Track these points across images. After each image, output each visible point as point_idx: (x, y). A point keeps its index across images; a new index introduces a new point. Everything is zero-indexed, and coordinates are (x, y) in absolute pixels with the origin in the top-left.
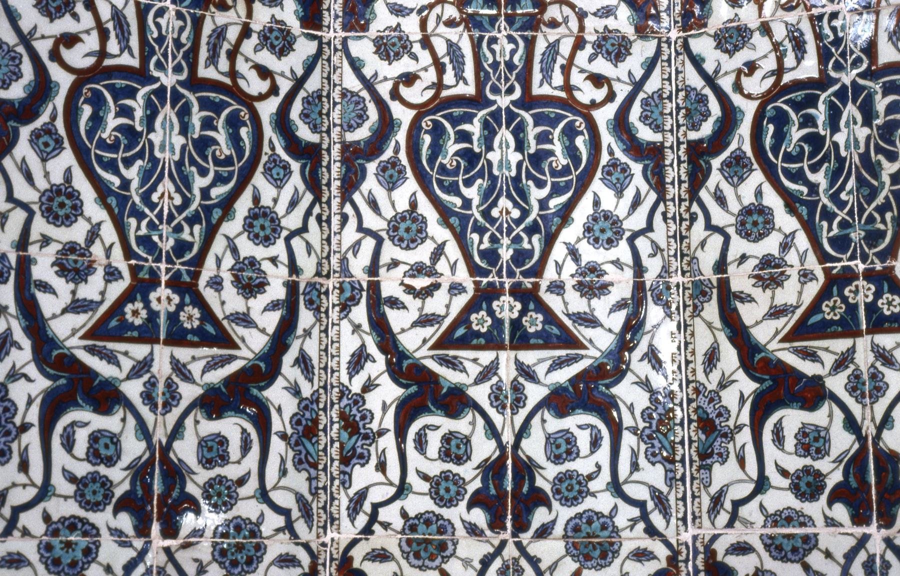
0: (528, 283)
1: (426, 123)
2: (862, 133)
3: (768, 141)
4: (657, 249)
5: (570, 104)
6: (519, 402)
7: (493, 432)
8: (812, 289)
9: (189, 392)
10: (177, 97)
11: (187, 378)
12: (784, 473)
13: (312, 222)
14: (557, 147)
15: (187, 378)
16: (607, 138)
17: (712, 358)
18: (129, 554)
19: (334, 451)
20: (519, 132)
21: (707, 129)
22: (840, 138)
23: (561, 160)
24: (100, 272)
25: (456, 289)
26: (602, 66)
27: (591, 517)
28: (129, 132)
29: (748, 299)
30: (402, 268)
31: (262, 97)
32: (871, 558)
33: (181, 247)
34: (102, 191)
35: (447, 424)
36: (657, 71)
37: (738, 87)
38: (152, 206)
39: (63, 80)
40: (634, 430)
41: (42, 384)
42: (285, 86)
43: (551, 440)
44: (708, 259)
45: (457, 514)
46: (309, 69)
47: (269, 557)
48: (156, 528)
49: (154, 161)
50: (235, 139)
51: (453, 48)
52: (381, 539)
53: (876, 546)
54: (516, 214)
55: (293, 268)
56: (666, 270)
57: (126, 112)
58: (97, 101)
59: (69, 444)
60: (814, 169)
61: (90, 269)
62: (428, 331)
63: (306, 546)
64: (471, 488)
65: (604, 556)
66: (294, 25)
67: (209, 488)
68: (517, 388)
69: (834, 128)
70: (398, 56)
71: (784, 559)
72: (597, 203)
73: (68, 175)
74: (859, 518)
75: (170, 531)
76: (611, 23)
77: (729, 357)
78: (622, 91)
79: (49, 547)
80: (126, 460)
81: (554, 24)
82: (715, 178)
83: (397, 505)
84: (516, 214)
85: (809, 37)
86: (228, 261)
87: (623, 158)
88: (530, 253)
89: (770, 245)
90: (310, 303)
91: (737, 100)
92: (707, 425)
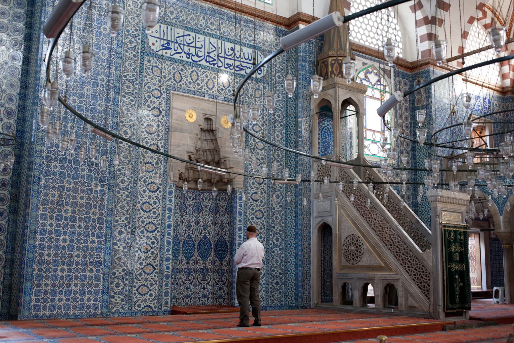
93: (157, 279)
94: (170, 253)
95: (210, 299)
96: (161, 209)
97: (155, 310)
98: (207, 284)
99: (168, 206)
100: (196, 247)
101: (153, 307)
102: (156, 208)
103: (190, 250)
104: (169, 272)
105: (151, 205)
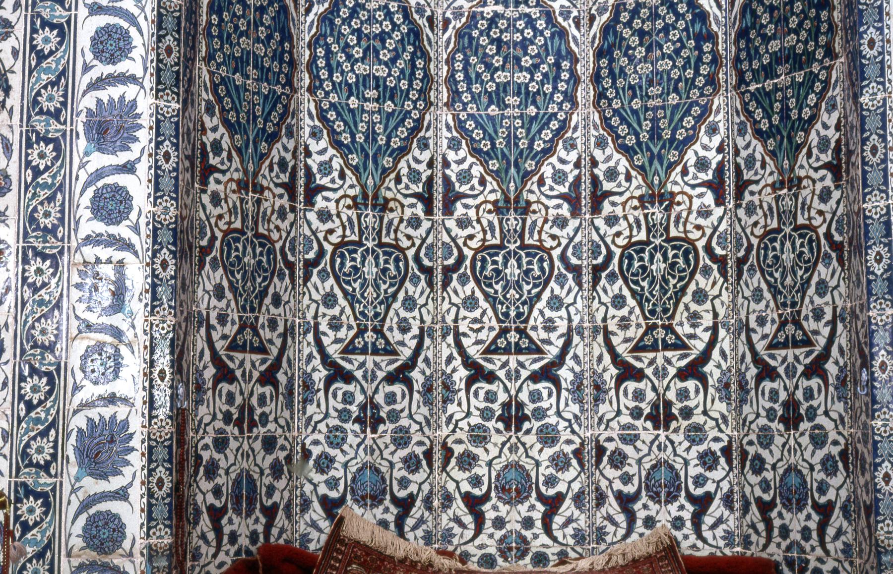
0: (522, 326)
1: (479, 257)
2: (663, 266)
3: (625, 267)
4: (578, 311)
5: (541, 248)
6: (518, 377)
7: (506, 390)
8: (641, 331)
9: (381, 375)
10: (374, 251)
11: (380, 369)
12: (627, 408)
13: (430, 300)
14: (536, 267)
15: (380, 369)
16: (557, 263)
17: (600, 359)
18: (359, 440)
19: (440, 398)
20: (519, 260)
21: (600, 260)
22: (654, 267)
23: (537, 273)
24: (345, 326)
25: (491, 329)
26: (556, 231)
27: (547, 426)
28: (355, 268)
29: (615, 334)
30: (468, 320)
31: (408, 248)
32: (660, 444)
33: (377, 315)
34: (345, 293)
35: (487, 387)
36: (579, 234)
37: (613, 242)
38: (365, 298)
39: (329, 248)
40: (567, 390)
41: (325, 373)
42: (418, 242)
43: (531, 394)
44: (599, 316)
45: (491, 424)
46: (428, 233)
47: (413, 442)
48: (368, 430)
49: (365, 279)
50: (397, 268)
51: (490, 224)
52: (459, 435)
53: (662, 439)
54: (517, 296)
55: (422, 321)
56: (582, 320)
57: (353, 259)
58: (342, 256)
59: (335, 396)
60: (643, 280)
61: (341, 326)
62: (479, 347)
63: (428, 437)
64: (498, 414)
65: (553, 442)
66: (422, 215)
67: (389, 413)
68: (517, 371)
69: (652, 263)
70: (466, 227)
71: (627, 444)
72: (552, 291)
73: (332, 287)
74: (656, 427)
75: (374, 431)
76: (560, 211)
77: (607, 358)
78: (564, 242)
79: (329, 437)
80: (357, 403)
81: (534, 212)
82: (603, 282)
83: (466, 420)
84: (517, 296)
85: (643, 222)
86: (396, 320)
87: (564, 272)
88: (523, 314)
89: (624, 312)
90: (429, 335)
91: (613, 247)
92: (597, 387)
94: (133, 65)
95: (716, 509)
100: (585, 69)
103: (529, 97)
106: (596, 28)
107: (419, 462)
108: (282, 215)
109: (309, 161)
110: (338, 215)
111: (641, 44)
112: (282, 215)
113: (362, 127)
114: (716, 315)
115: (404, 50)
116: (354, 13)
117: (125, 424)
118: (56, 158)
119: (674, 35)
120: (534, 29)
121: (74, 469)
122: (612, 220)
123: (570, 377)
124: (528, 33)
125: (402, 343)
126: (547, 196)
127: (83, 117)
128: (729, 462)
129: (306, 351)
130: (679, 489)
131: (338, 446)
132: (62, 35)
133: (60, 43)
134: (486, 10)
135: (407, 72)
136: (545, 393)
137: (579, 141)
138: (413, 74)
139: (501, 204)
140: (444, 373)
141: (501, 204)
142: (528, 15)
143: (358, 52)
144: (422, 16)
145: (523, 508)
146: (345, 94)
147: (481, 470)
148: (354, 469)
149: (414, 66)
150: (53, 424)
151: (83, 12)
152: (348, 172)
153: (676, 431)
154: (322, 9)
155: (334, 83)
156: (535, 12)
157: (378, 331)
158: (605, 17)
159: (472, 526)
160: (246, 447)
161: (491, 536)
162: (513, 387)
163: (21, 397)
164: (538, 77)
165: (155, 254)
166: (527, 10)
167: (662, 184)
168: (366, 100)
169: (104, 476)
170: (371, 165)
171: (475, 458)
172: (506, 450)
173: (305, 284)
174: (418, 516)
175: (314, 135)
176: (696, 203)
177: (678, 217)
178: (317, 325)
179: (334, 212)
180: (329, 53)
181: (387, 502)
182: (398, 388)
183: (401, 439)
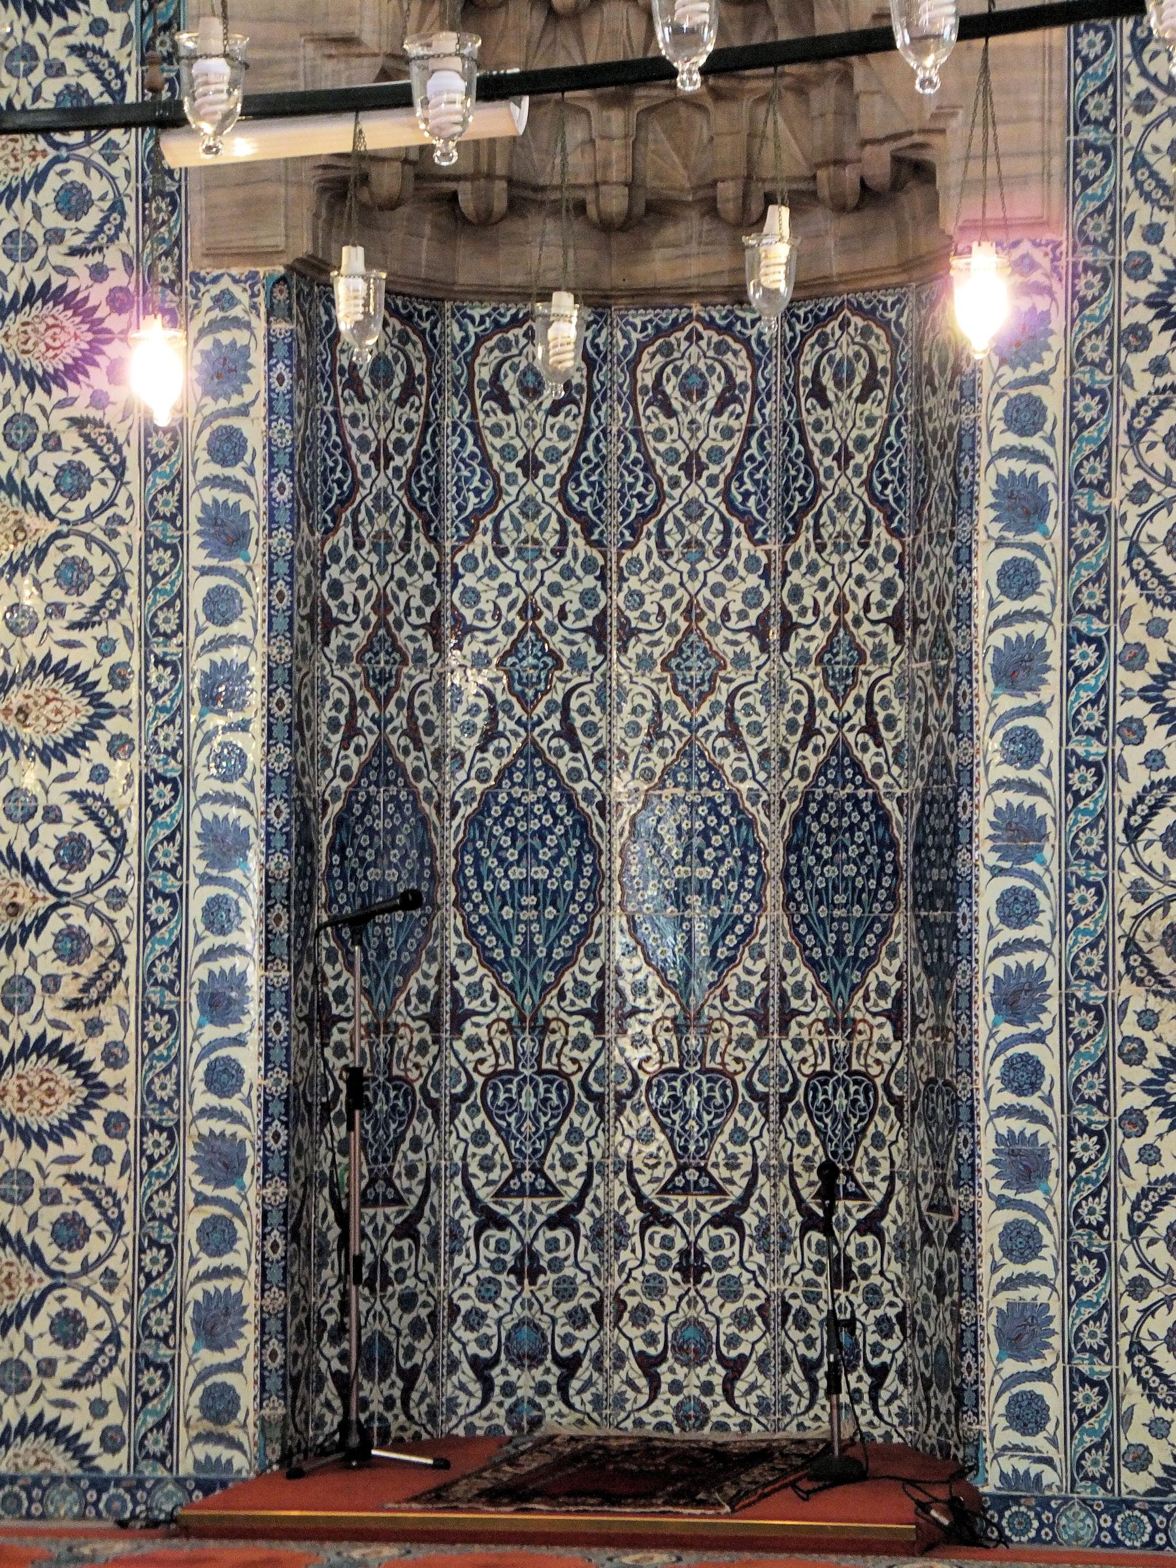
6: (697, 1221)
11: (539, 1211)
18: (514, 1293)
21: (787, 1089)
25: (668, 1165)
26: (740, 1053)
28: (510, 1101)
33: (535, 1151)
35: (663, 1231)
39: (479, 1080)
41: (474, 1219)
44: (785, 1153)
45: (667, 1274)
46: (598, 1055)
50: (561, 1097)
55: (590, 1155)
57: (508, 1091)
59: (487, 1245)
68: (697, 1214)
75: (533, 1282)
78: (750, 1066)
93: (122, 1186)
95: (892, 1382)
96: (133, 532)
97: (108, 1463)
98: (717, 1221)
99: (209, 495)
100: (774, 863)
101: (92, 1438)
102: (94, 528)
104: (236, 1118)
105: (41, 506)
106: (786, 817)
107: (587, 1316)
108: (422, 1048)
109: (456, 984)
110: (490, 1042)
111: (828, 843)
112: (422, 1048)
113: (518, 939)
114: (892, 1163)
115: (569, 845)
116: (507, 810)
117: (239, 1295)
118: (171, 1030)
119: (859, 837)
120: (719, 816)
121: (190, 1340)
122: (798, 1044)
123: (755, 1221)
124: (712, 821)
125: (566, 1182)
126: (732, 1013)
127: (196, 989)
128: (903, 1331)
129: (454, 1196)
130: (857, 1358)
131: (491, 1300)
132: (174, 905)
133: (173, 913)
134: (665, 792)
135: (573, 871)
136: (727, 1240)
137: (767, 949)
138: (579, 871)
139: (680, 1021)
140: (616, 1214)
141: (680, 1021)
142: (711, 800)
143: (512, 855)
144: (590, 803)
145: (702, 1371)
146: (498, 904)
147: (656, 1327)
148: (509, 1326)
149: (581, 863)
150: (172, 1296)
151: (194, 882)
152: (501, 992)
153: (855, 1291)
154: (470, 810)
155: (484, 893)
156: (719, 797)
157: (538, 1171)
158: (795, 805)
159: (646, 1390)
160: (378, 1307)
161: (667, 1402)
162: (692, 1234)
163: (141, 1269)
164: (723, 871)
165: (266, 1126)
166: (711, 794)
167: (845, 1009)
168: (522, 908)
169: (220, 1349)
170: (529, 983)
171: (650, 1312)
172: (684, 1304)
173: (452, 1122)
174: (586, 1376)
175: (460, 954)
176: (877, 1034)
177: (860, 1048)
178: (466, 1166)
179: (485, 1038)
180: (478, 860)
181: (548, 1363)
182: (561, 1233)
183: (565, 1290)
